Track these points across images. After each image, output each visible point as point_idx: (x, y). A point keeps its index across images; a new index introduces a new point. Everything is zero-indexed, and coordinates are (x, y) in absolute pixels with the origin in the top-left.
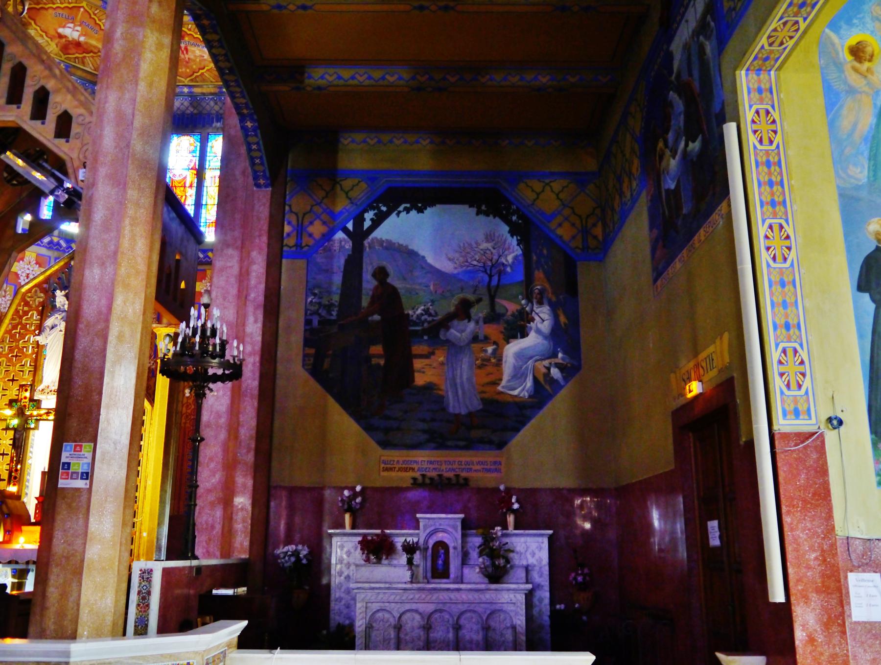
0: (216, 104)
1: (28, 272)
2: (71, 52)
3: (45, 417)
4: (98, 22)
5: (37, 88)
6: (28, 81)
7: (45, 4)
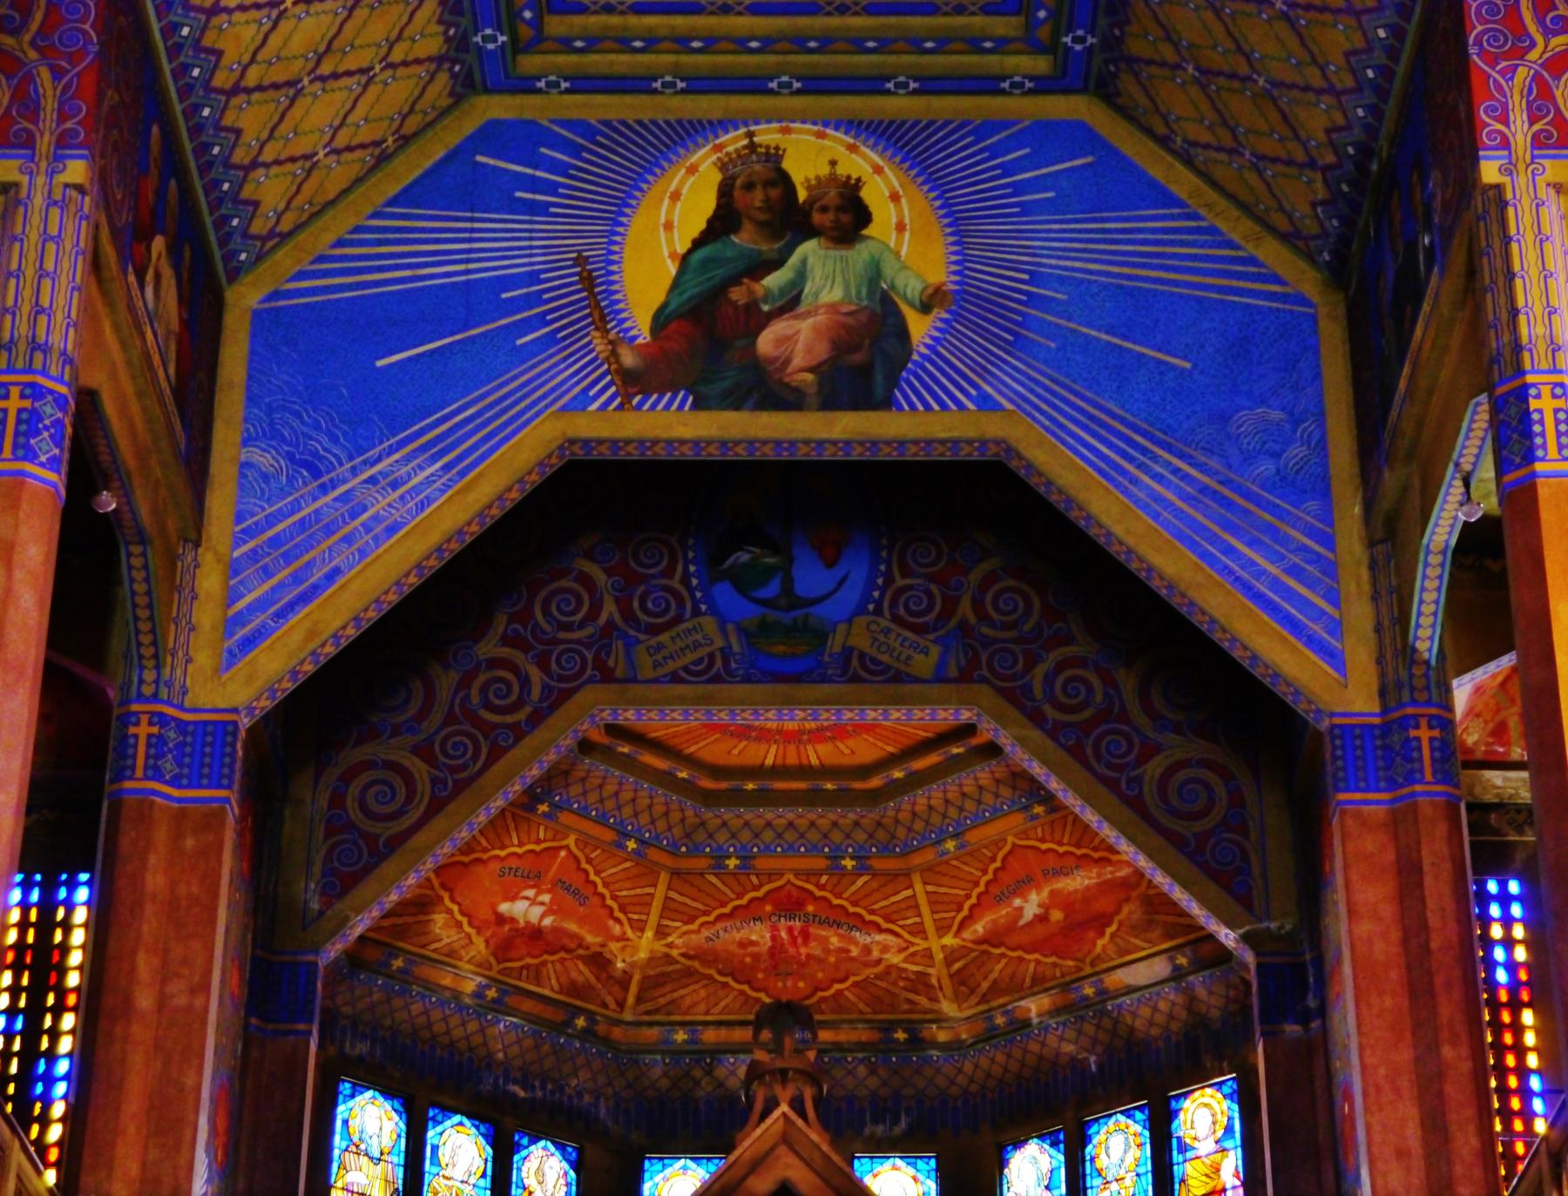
0: (873, 1072)
2: (514, 954)
4: (592, 877)
7: (485, 850)
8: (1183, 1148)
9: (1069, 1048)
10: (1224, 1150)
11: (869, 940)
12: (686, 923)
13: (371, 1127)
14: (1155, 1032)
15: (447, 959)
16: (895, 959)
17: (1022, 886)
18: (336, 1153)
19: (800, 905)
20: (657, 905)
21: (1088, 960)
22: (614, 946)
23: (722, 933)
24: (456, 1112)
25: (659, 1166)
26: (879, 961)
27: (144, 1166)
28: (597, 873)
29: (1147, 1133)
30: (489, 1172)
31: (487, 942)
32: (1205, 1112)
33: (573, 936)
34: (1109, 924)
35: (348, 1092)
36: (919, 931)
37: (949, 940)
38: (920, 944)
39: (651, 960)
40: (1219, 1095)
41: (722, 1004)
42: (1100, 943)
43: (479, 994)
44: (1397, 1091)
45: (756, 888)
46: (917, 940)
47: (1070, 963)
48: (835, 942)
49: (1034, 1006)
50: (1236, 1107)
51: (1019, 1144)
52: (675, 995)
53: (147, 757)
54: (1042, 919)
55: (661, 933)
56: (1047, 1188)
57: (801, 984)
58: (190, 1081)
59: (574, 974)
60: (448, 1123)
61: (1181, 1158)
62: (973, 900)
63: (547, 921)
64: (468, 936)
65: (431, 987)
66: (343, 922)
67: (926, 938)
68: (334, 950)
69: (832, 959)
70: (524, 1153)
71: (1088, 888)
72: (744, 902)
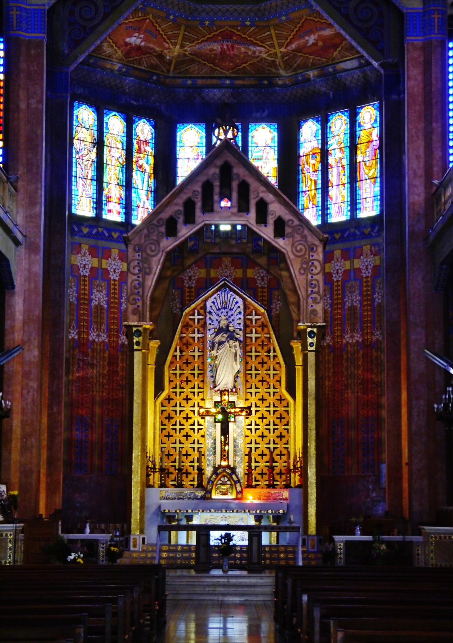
1: (114, 267)
3: (240, 413)
4: (158, 28)
5: (257, 199)
6: (252, 196)
8: (360, 126)
9: (323, 89)
10: (374, 127)
11: (255, 49)
12: (191, 43)
13: (85, 118)
14: (352, 85)
15: (109, 59)
16: (264, 56)
17: (309, 32)
18: (74, 127)
19: (231, 37)
20: (180, 37)
21: (331, 59)
22: (166, 51)
23: (203, 47)
24: (113, 111)
25: (182, 127)
26: (258, 57)
27: (27, 160)
28: (160, 26)
29: (348, 120)
30: (125, 131)
31: (122, 52)
32: (368, 114)
33: (152, 49)
34: (338, 48)
35: (77, 106)
36: (272, 46)
37: (283, 50)
38: (273, 51)
39: (179, 56)
40: (373, 109)
41: (204, 71)
42: (335, 53)
43: (120, 70)
44: (418, 136)
45: (215, 31)
46: (272, 49)
47: (325, 60)
48: (243, 50)
49: (312, 74)
50: (378, 113)
51: (305, 121)
52: (187, 68)
53: (17, 22)
54: (315, 44)
55: (182, 46)
56: (315, 137)
57: (231, 64)
58: (39, 132)
59: (152, 61)
60: (111, 115)
61: (359, 129)
62: (291, 37)
63: (143, 44)
64: (116, 50)
65: (104, 69)
66: (76, 58)
67: (275, 49)
68: (73, 67)
69: (242, 56)
70: (137, 124)
71: (331, 35)
72: (211, 36)
